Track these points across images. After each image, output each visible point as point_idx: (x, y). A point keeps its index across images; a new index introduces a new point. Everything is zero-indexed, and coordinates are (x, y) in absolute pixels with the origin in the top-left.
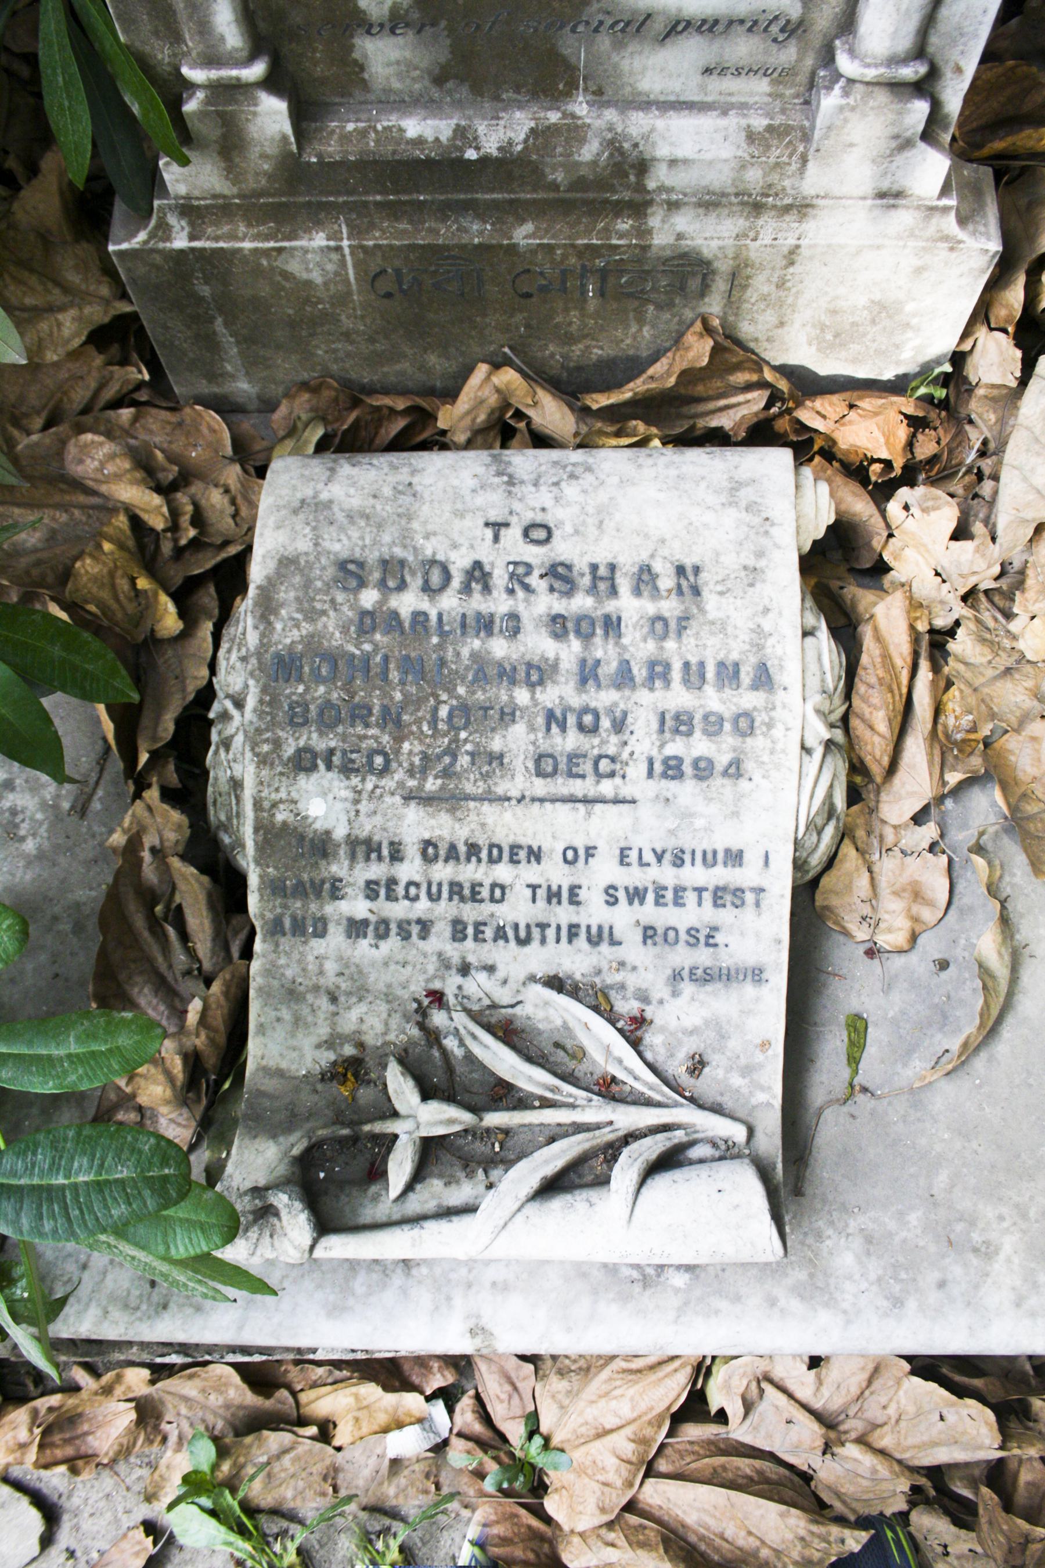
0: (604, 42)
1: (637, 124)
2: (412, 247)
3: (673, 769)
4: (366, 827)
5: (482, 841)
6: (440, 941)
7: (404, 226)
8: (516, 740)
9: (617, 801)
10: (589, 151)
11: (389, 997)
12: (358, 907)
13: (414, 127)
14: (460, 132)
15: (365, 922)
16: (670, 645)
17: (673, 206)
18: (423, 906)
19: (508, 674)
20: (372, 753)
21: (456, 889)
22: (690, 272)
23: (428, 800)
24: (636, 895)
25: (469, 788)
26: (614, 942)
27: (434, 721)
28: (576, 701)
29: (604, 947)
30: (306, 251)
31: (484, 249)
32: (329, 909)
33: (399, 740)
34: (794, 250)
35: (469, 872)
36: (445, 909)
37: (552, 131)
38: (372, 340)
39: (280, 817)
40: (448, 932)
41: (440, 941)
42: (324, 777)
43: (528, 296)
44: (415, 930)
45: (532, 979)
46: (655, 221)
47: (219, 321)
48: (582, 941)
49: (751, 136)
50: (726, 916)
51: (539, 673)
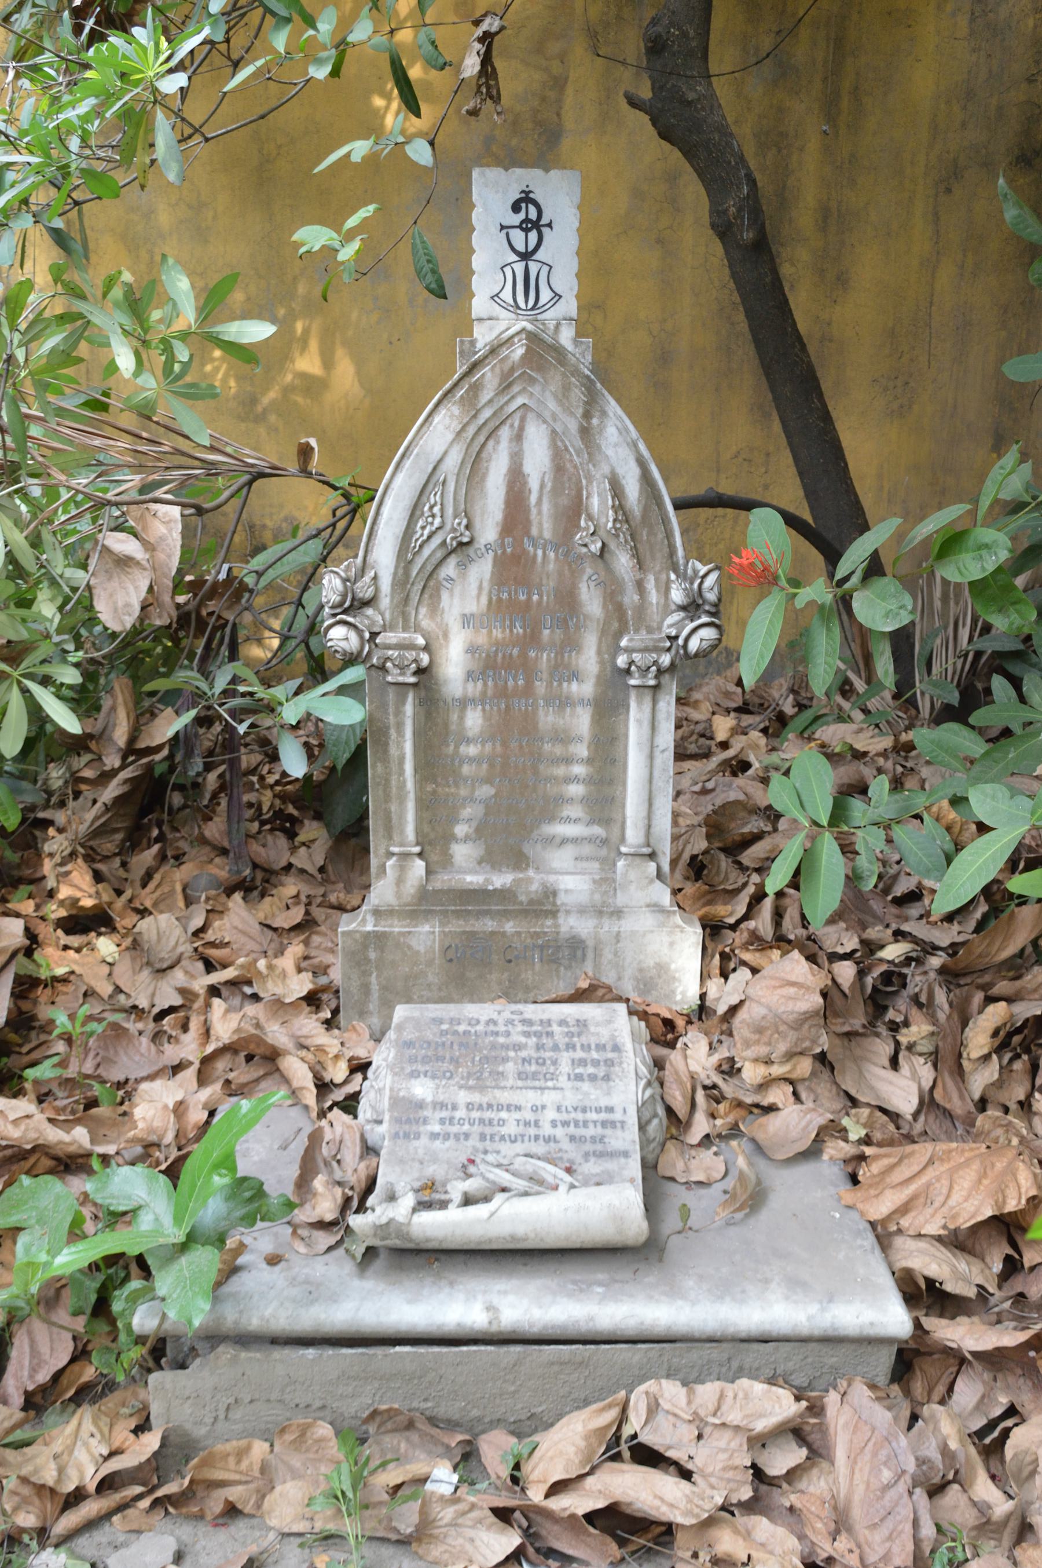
0: (539, 846)
1: (552, 878)
2: (464, 932)
3: (579, 1078)
4: (441, 1098)
5: (494, 1103)
6: (474, 1142)
7: (461, 922)
8: (510, 1067)
9: (555, 1088)
10: (534, 887)
11: (448, 1162)
12: (437, 1128)
13: (469, 878)
14: (487, 880)
15: (438, 1134)
16: (575, 1039)
17: (568, 912)
18: (466, 1127)
19: (506, 1047)
20: (444, 1073)
21: (482, 1121)
22: (576, 947)
23: (470, 1088)
24: (565, 1124)
25: (488, 1084)
26: (556, 1141)
27: (473, 1061)
28: (535, 1055)
29: (552, 1144)
30: (420, 933)
31: (493, 933)
32: (422, 1129)
33: (457, 1068)
34: (618, 933)
35: (488, 1115)
36: (477, 1129)
37: (520, 880)
38: (440, 989)
39: (401, 1094)
40: (478, 1138)
41: (474, 1142)
42: (422, 1079)
43: (510, 961)
44: (462, 1137)
45: (518, 1155)
46: (561, 921)
47: (374, 975)
48: (541, 1141)
49: (594, 881)
50: (608, 1132)
51: (518, 1047)
